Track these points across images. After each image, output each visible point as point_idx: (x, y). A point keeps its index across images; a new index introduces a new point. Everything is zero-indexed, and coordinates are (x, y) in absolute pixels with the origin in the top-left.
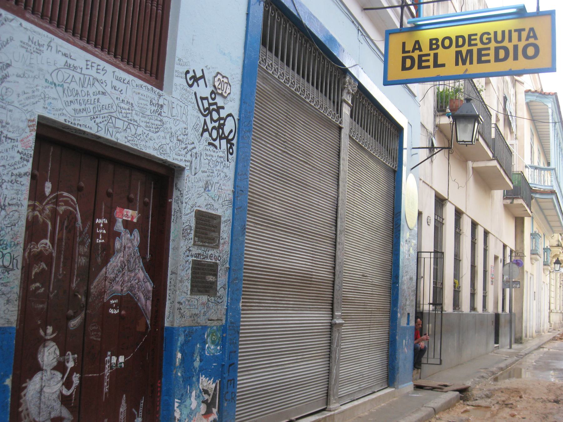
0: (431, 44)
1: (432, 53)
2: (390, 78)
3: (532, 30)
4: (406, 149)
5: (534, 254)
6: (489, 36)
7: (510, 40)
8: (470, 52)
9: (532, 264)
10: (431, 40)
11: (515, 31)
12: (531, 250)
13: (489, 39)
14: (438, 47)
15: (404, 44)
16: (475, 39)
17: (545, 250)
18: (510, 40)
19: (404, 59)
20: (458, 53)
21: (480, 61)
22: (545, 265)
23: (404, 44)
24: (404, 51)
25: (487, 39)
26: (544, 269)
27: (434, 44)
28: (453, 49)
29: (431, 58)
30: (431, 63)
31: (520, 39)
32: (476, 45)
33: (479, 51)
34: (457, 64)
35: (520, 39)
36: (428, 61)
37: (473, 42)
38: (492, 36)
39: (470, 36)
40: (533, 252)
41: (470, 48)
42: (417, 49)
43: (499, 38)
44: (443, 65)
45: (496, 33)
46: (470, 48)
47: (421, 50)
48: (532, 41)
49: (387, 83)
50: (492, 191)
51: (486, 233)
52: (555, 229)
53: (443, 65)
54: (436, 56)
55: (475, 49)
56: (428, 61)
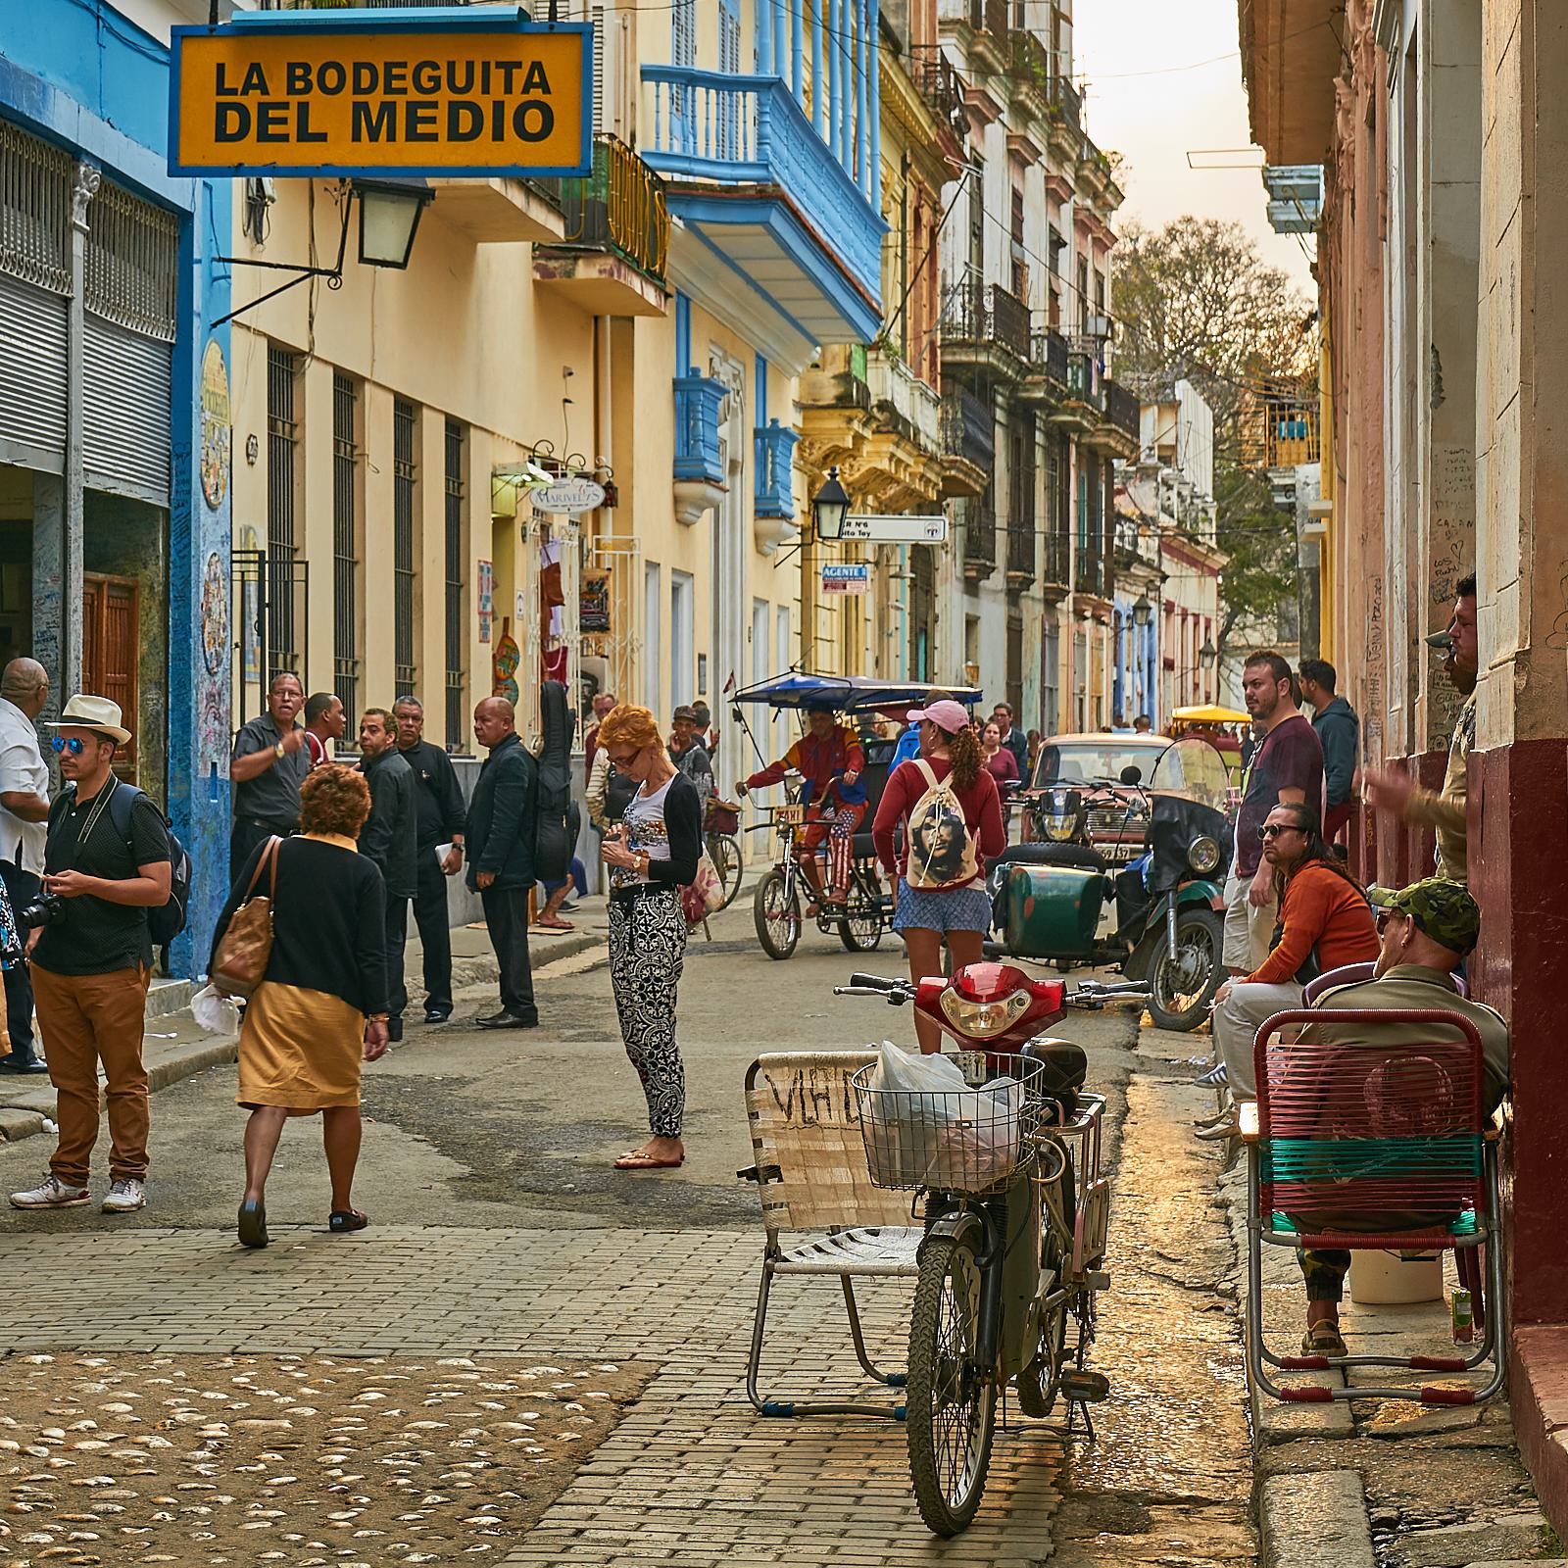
0: (292, 79)
1: (294, 100)
2: (185, 160)
3: (537, 66)
4: (199, 261)
5: (689, 479)
6: (436, 73)
7: (486, 90)
8: (388, 108)
9: (684, 524)
10: (291, 67)
11: (499, 65)
12: (676, 462)
13: (437, 80)
14: (307, 89)
15: (221, 67)
16: (403, 77)
17: (768, 436)
18: (486, 90)
19: (222, 110)
20: (360, 108)
21: (412, 136)
22: (762, 514)
23: (221, 67)
24: (221, 90)
25: (430, 78)
26: (757, 537)
27: (299, 78)
28: (347, 96)
29: (292, 114)
30: (292, 128)
31: (508, 90)
32: (404, 91)
33: (412, 107)
34: (356, 137)
35: (508, 90)
36: (283, 121)
37: (395, 84)
38: (443, 73)
39: (388, 66)
40: (685, 469)
41: (390, 98)
42: (255, 87)
43: (460, 82)
44: (322, 137)
45: (451, 65)
46: (390, 98)
47: (265, 92)
48: (536, 94)
49: (175, 170)
50: (483, 248)
51: (457, 430)
52: (813, 328)
53: (322, 137)
54: (303, 108)
55: (401, 101)
56: (283, 121)
